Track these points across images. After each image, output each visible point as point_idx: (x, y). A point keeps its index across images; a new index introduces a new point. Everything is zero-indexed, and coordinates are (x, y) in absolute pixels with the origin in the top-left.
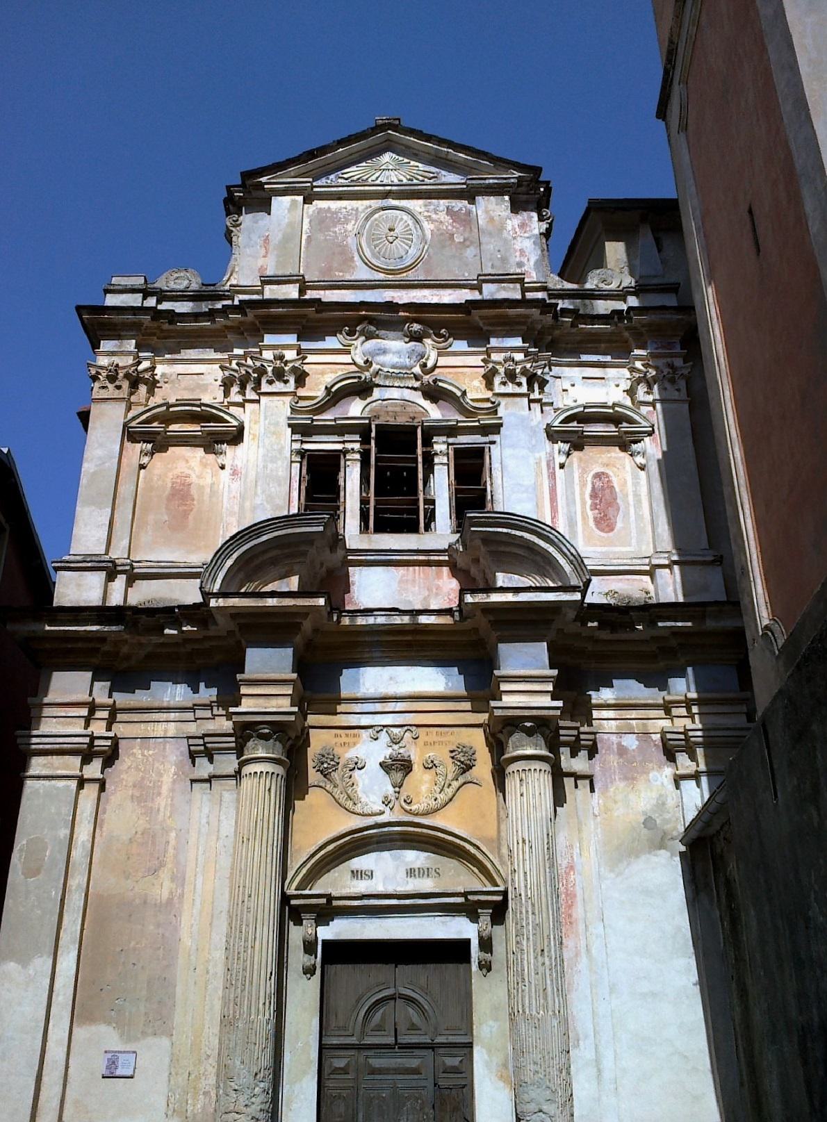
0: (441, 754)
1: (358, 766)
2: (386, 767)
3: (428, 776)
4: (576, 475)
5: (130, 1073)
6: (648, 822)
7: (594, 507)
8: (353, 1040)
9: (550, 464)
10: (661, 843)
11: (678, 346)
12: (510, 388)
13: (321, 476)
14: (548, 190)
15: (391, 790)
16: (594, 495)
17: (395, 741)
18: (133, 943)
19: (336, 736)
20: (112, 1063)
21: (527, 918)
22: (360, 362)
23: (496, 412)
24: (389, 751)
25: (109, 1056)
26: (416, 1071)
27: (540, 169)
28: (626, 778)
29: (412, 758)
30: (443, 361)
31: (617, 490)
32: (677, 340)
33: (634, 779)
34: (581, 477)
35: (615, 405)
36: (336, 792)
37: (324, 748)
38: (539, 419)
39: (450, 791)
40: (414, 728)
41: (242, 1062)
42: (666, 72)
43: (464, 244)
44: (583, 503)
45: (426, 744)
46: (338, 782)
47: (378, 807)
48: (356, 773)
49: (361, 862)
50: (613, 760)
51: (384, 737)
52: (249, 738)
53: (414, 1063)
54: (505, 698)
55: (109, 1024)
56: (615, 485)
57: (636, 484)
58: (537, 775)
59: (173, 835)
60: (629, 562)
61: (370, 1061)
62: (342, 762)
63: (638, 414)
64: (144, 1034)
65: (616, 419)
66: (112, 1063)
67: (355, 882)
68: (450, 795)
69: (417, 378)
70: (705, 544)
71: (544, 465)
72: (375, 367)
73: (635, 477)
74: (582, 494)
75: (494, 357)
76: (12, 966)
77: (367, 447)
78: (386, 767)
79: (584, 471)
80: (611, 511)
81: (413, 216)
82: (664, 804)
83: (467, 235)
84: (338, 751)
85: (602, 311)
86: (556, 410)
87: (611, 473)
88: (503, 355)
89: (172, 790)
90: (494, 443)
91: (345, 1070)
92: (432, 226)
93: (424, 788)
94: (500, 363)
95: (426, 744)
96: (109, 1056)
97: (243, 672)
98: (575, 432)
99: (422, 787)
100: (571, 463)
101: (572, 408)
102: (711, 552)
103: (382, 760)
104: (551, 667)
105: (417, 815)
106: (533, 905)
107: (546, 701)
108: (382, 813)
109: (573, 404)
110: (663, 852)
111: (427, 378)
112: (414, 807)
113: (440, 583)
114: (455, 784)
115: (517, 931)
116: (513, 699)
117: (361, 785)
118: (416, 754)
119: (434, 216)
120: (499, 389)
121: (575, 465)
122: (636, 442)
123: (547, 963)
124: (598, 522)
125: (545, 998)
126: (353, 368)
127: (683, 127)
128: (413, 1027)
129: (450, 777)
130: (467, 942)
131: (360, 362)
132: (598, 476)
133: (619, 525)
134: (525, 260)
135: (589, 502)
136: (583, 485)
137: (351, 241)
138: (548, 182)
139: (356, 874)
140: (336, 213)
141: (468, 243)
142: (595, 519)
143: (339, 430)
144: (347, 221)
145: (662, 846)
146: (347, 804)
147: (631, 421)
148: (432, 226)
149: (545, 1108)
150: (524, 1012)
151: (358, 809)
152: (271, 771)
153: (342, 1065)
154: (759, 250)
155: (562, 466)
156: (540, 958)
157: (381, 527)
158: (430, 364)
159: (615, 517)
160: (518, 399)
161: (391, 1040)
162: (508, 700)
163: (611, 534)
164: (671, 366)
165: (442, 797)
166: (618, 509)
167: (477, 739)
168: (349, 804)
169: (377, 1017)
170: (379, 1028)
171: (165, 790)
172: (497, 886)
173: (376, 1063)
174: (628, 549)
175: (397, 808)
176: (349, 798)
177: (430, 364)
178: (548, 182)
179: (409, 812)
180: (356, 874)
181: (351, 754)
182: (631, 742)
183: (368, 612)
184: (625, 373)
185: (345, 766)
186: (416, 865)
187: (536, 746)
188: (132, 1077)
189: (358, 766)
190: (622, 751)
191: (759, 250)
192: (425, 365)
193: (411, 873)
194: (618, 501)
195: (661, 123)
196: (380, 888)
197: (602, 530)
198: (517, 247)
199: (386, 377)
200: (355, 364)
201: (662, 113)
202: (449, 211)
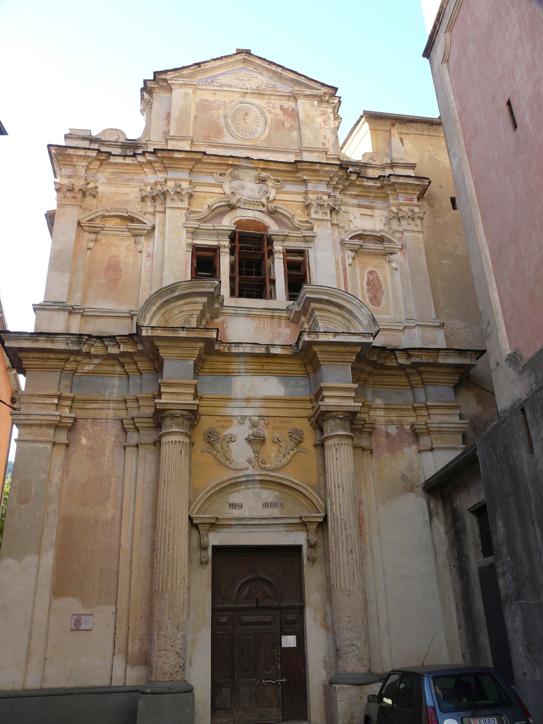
0: (283, 435)
1: (232, 439)
2: (249, 441)
3: (275, 448)
4: (358, 271)
5: (88, 627)
6: (404, 477)
7: (369, 291)
8: (231, 605)
9: (344, 262)
10: (411, 489)
11: (416, 200)
12: (320, 216)
13: (204, 262)
14: (340, 102)
15: (252, 455)
16: (368, 284)
17: (254, 425)
18: (89, 547)
19: (217, 421)
20: (78, 623)
21: (342, 531)
22: (228, 192)
23: (312, 229)
24: (251, 432)
25: (75, 617)
26: (269, 623)
27: (336, 89)
28: (389, 451)
29: (266, 436)
30: (279, 197)
31: (382, 282)
32: (415, 197)
33: (395, 451)
34: (361, 273)
35: (380, 231)
36: (219, 456)
37: (210, 428)
38: (337, 236)
39: (288, 457)
40: (265, 418)
41: (169, 619)
42: (435, 27)
43: (291, 129)
44: (363, 288)
45: (273, 428)
46: (220, 449)
47: (245, 464)
48: (231, 445)
49: (235, 497)
50: (383, 440)
51: (247, 423)
52: (163, 418)
53: (268, 619)
54: (326, 400)
55: (75, 597)
56: (381, 279)
57: (392, 279)
58: (346, 446)
59: (114, 479)
60: (389, 324)
61: (243, 618)
62: (221, 437)
63: (394, 237)
64: (98, 603)
65: (381, 239)
66: (78, 623)
67: (231, 510)
68: (289, 459)
69: (263, 205)
70: (434, 316)
71: (340, 263)
72: (238, 197)
73: (392, 275)
74: (362, 283)
75: (310, 196)
76: (10, 562)
77: (233, 244)
78: (249, 441)
79: (363, 269)
80: (378, 295)
81: (260, 109)
82: (412, 467)
83: (293, 123)
84: (218, 430)
85: (371, 176)
86: (346, 232)
87: (378, 272)
88: (316, 196)
89: (113, 452)
90: (310, 247)
91: (226, 624)
92: (271, 116)
93: (273, 455)
94: (314, 201)
95: (273, 428)
96: (75, 617)
97: (162, 378)
98: (363, 243)
99: (271, 452)
100: (355, 265)
101: (356, 231)
102: (437, 320)
103: (246, 437)
104: (353, 382)
105: (269, 470)
106: (345, 524)
107: (351, 403)
108: (247, 469)
109: (355, 229)
110: (411, 494)
111: (271, 206)
112: (267, 466)
113: (280, 330)
114: (292, 453)
115: (335, 539)
116: (331, 402)
117: (233, 451)
118: (267, 433)
119: (272, 110)
120: (313, 216)
121: (357, 265)
122: (391, 254)
123: (354, 558)
124: (371, 300)
125: (354, 578)
126: (223, 196)
127: (446, 60)
128: (268, 597)
129: (289, 448)
130: (299, 548)
131: (228, 192)
132: (371, 272)
133: (383, 302)
134: (326, 142)
135: (366, 288)
136: (362, 278)
137: (222, 120)
138: (340, 98)
139: (232, 506)
140: (212, 103)
141: (293, 128)
142: (370, 297)
143: (218, 233)
144: (219, 108)
145: (411, 491)
146: (225, 462)
147: (390, 241)
148: (271, 116)
149: (355, 643)
150: (341, 587)
151: (233, 466)
152: (181, 440)
153: (225, 620)
154: (515, 126)
155: (350, 265)
156: (350, 555)
157: (241, 296)
158: (271, 197)
159: (381, 297)
160: (325, 223)
161: (254, 605)
162: (327, 401)
163: (379, 307)
164: (412, 211)
165: (284, 461)
166: (383, 293)
167: (305, 426)
168: (227, 463)
169: (245, 593)
170: (247, 598)
171: (108, 452)
172: (320, 513)
173: (246, 619)
174: (389, 317)
175: (256, 466)
176: (227, 459)
177: (271, 197)
178: (340, 98)
179: (264, 469)
180: (232, 506)
181: (227, 432)
182: (393, 430)
183: (238, 344)
184: (385, 213)
185: (223, 440)
186: (269, 501)
187: (345, 429)
188: (91, 630)
189: (232, 439)
190: (388, 435)
191: (515, 126)
192: (268, 198)
193: (266, 505)
194: (383, 288)
195: (426, 61)
196: (247, 515)
197: (373, 305)
198: (323, 134)
199: (245, 203)
200: (224, 194)
201: (427, 53)
202: (282, 108)
